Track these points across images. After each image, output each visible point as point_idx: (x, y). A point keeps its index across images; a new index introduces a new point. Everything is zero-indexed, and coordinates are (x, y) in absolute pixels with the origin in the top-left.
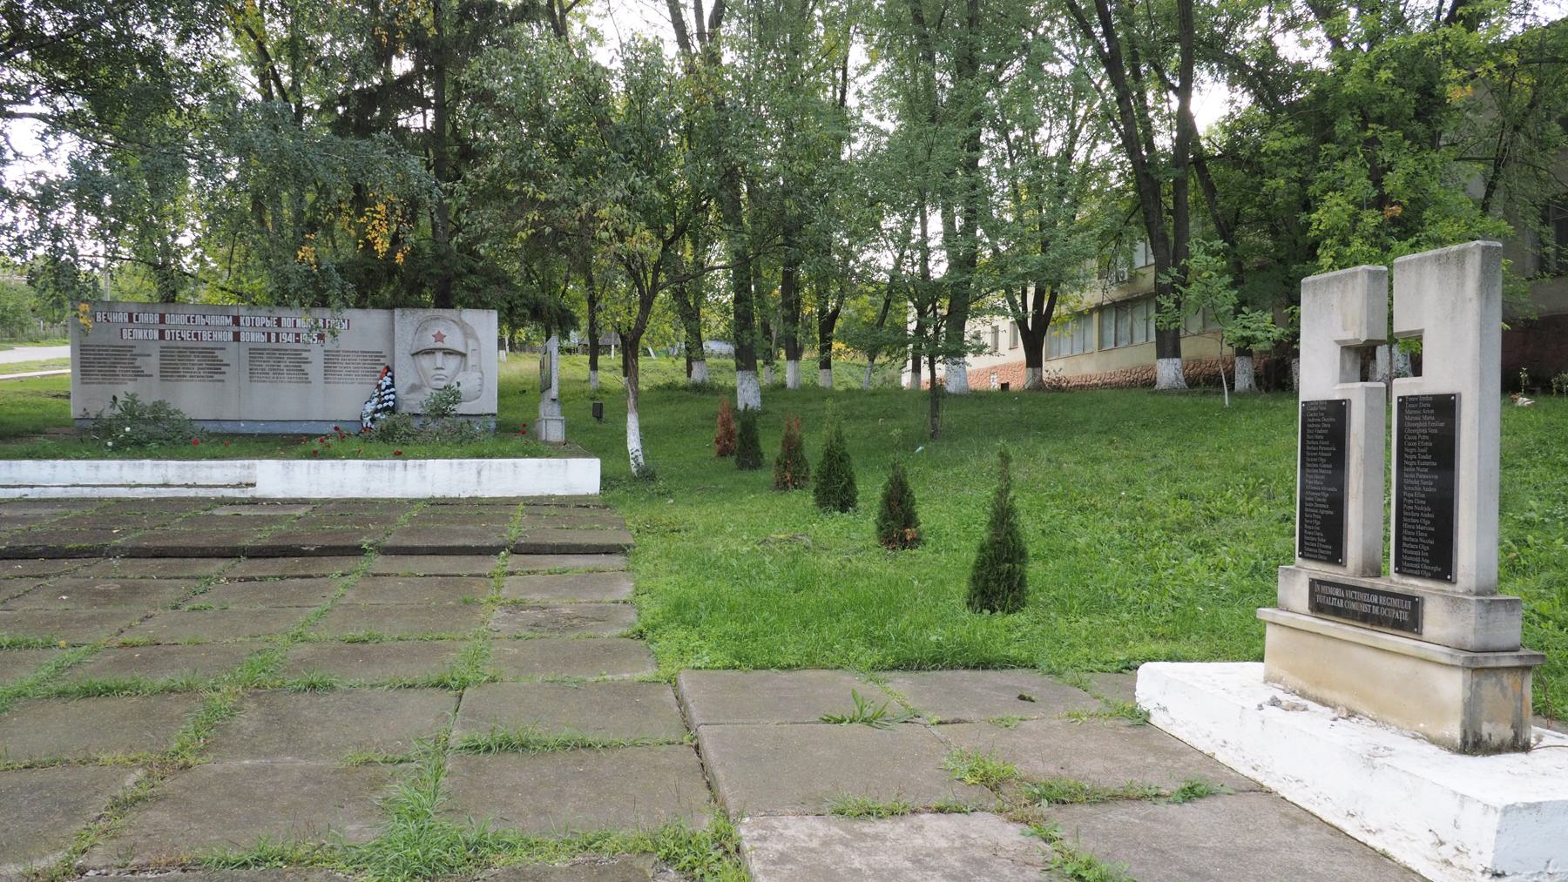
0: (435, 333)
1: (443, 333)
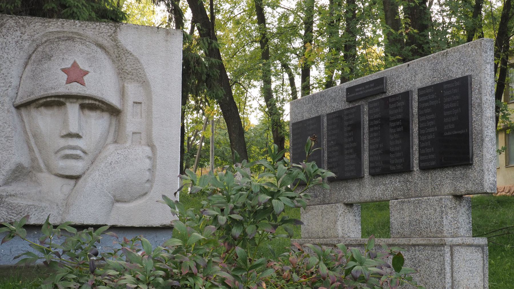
1: (83, 65)
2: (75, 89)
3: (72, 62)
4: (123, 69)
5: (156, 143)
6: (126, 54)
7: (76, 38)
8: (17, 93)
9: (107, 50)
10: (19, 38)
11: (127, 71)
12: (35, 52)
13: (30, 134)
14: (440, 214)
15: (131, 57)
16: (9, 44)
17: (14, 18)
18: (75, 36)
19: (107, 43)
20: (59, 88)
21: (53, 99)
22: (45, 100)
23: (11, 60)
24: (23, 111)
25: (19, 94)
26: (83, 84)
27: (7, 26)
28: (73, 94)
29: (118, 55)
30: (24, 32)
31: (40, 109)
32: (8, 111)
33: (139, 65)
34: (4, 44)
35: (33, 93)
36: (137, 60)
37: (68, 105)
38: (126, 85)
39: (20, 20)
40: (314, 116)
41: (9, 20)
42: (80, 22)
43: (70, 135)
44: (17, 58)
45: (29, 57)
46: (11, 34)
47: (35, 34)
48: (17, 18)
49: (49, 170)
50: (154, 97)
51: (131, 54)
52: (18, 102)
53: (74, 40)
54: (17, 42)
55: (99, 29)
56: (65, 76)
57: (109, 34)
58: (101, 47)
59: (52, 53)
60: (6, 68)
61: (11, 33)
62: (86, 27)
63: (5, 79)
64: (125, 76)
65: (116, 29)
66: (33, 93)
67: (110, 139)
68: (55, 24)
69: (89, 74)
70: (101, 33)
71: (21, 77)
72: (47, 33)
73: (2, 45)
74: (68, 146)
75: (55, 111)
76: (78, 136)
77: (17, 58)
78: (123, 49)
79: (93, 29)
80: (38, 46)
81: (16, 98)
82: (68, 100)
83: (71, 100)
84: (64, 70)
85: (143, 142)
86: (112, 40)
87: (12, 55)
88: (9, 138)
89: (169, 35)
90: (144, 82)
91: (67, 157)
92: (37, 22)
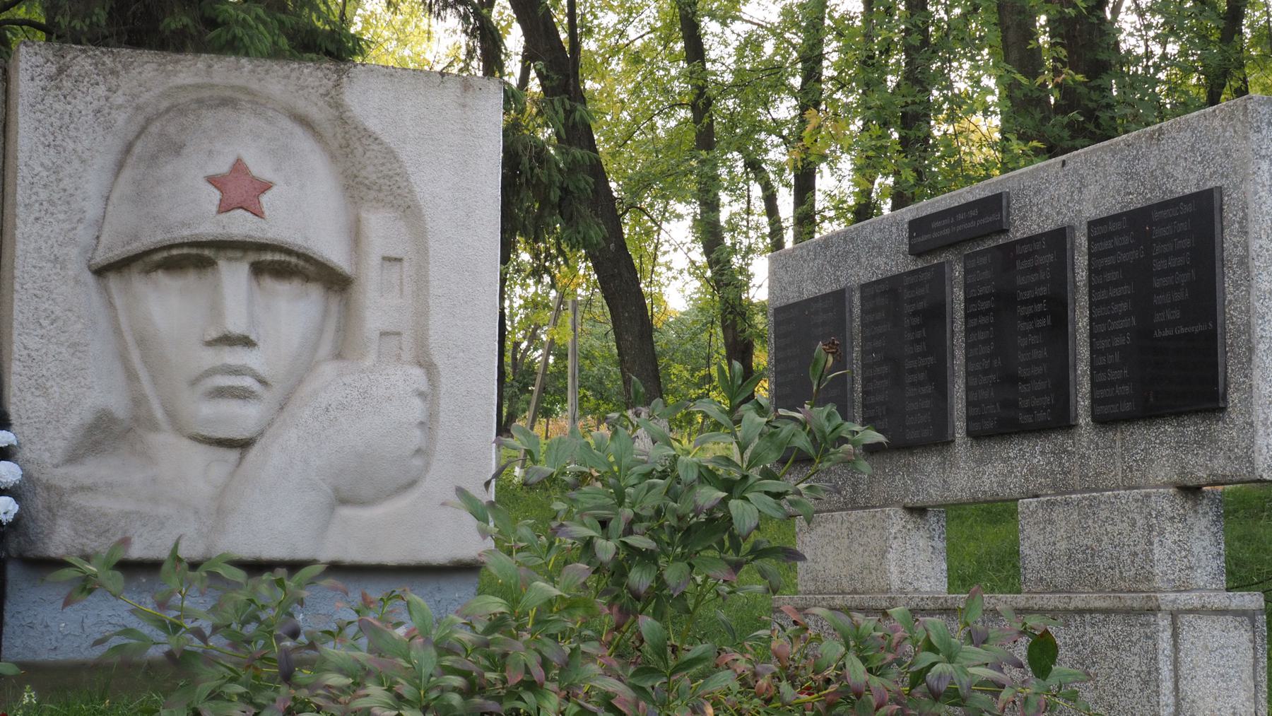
0: (221, 166)
1: (260, 167)
2: (240, 225)
3: (231, 160)
4: (356, 177)
5: (439, 360)
6: (364, 140)
7: (240, 100)
8: (98, 237)
9: (318, 129)
10: (102, 102)
11: (367, 182)
12: (143, 136)
13: (129, 338)
14: (1146, 533)
15: (376, 147)
16: (78, 115)
17: (91, 53)
18: (238, 95)
19: (317, 111)
20: (199, 224)
21: (185, 251)
22: (165, 254)
23: (84, 156)
24: (113, 281)
25: (103, 239)
26: (258, 214)
27: (75, 73)
28: (235, 239)
29: (344, 142)
30: (114, 88)
31: (153, 275)
32: (77, 282)
33: (395, 165)
34: (66, 117)
35: (136, 237)
36: (391, 155)
37: (222, 264)
38: (364, 215)
39: (105, 59)
40: (828, 290)
41: (79, 59)
42: (251, 62)
43: (228, 340)
44: (97, 151)
45: (128, 149)
46: (83, 93)
47: (141, 92)
48: (97, 52)
49: (176, 423)
50: (433, 245)
51: (376, 139)
52: (101, 258)
53: (236, 105)
54: (99, 112)
55: (299, 79)
56: (216, 195)
57: (322, 91)
58: (304, 121)
59: (184, 137)
60: (70, 176)
61: (85, 90)
62: (267, 72)
63: (68, 203)
64: (362, 194)
65: (340, 78)
66: (136, 237)
67: (326, 348)
68: (191, 66)
69: (274, 189)
70: (303, 88)
71: (108, 198)
72: (171, 88)
73: (61, 118)
74: (223, 365)
75: (190, 280)
76: (246, 342)
77: (97, 151)
78: (356, 128)
79: (285, 77)
80: (149, 121)
81: (95, 249)
82: (222, 254)
83: (230, 254)
84: (212, 180)
85: (407, 355)
86: (330, 106)
87: (87, 143)
88: (80, 348)
89: (471, 92)
90: (409, 207)
91: (221, 393)
92: (147, 62)
